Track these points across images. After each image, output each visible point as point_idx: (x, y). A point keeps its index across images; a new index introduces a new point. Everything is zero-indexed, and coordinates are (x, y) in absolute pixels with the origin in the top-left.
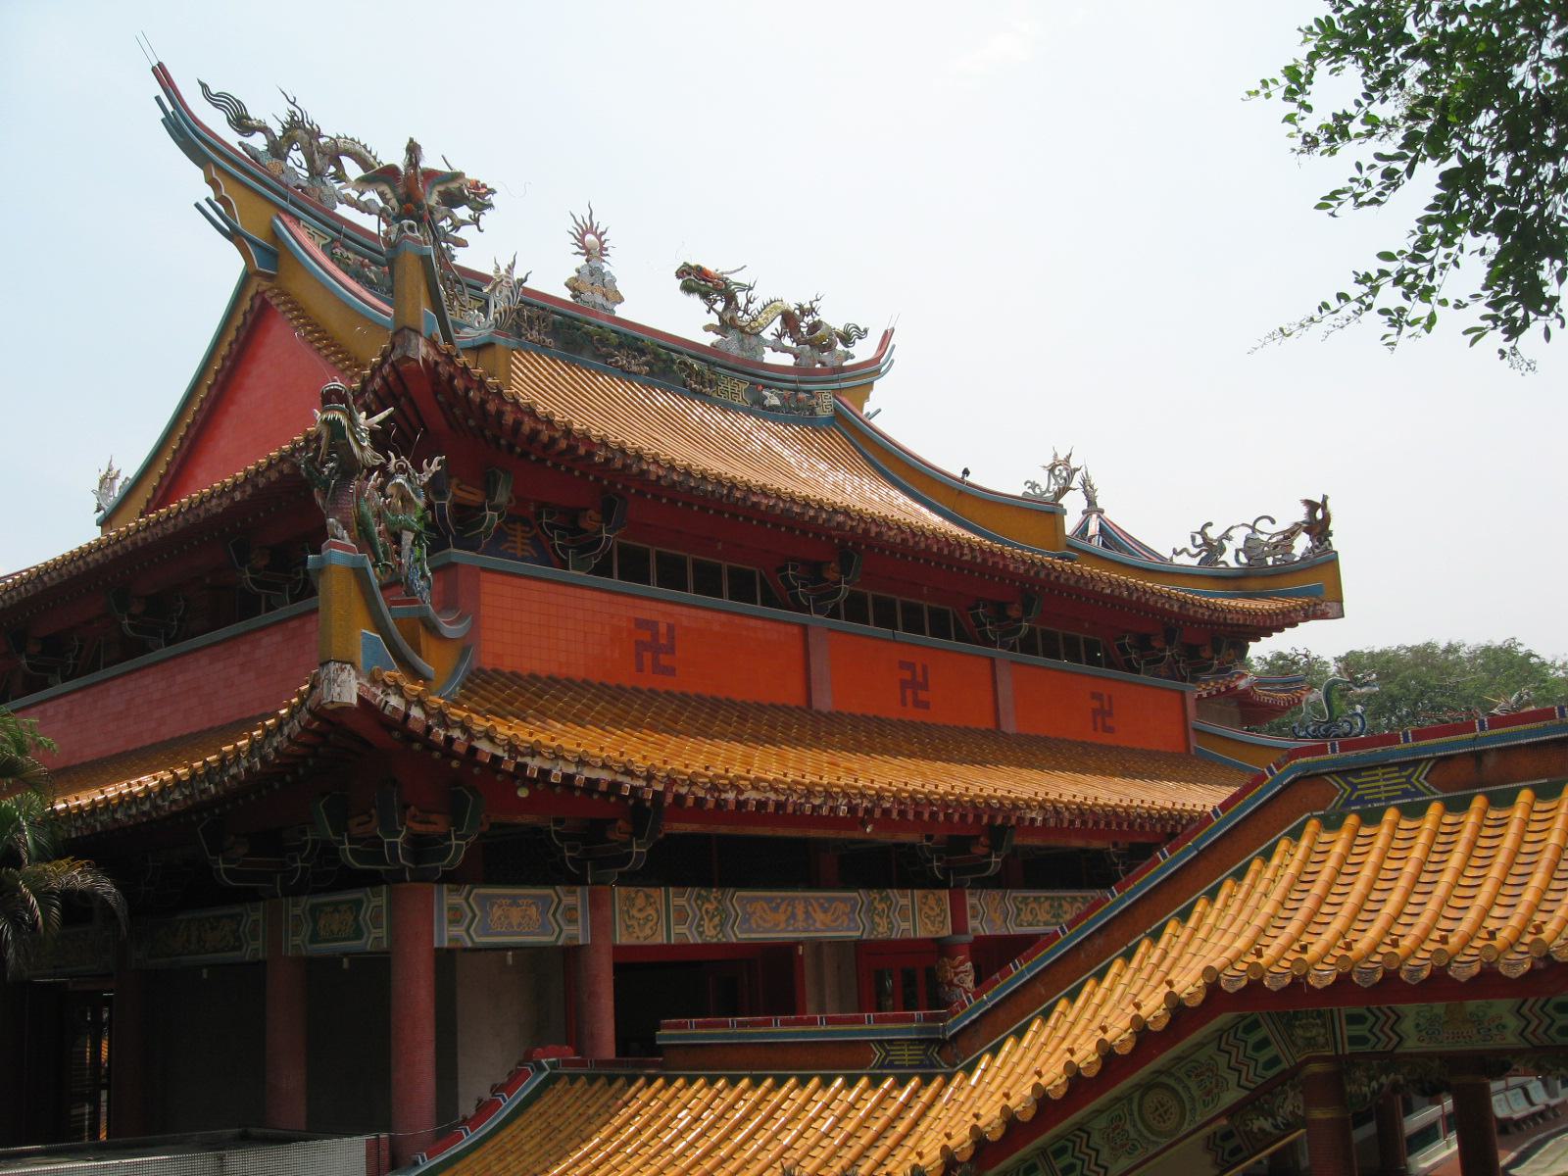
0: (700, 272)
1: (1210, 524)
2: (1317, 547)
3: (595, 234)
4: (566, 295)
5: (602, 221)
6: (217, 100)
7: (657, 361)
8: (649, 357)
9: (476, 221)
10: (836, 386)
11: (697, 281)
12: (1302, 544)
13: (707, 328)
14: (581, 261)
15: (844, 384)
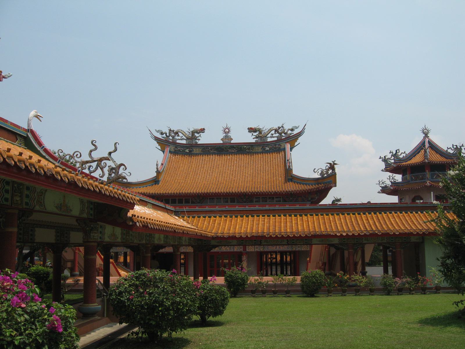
0: (251, 128)
3: (228, 129)
4: (222, 142)
5: (229, 126)
6: (158, 131)
8: (236, 149)
9: (200, 136)
11: (251, 130)
13: (254, 138)
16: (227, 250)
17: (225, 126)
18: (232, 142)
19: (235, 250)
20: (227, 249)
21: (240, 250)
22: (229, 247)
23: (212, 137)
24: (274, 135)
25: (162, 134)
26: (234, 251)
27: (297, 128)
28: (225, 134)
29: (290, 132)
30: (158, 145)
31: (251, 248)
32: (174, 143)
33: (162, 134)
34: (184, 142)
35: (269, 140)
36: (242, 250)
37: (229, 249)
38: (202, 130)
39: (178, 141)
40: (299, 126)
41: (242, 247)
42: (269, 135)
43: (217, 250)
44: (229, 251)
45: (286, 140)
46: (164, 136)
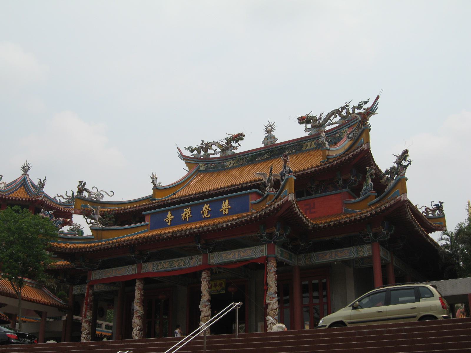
3: (270, 126)
4: (263, 145)
5: (271, 122)
6: (187, 149)
7: (296, 146)
10: (349, 125)
11: (302, 120)
14: (267, 135)
15: (352, 124)
16: (180, 266)
17: (266, 123)
18: (277, 142)
20: (180, 264)
21: (199, 263)
22: (183, 261)
23: (253, 142)
24: (333, 121)
25: (192, 150)
27: (365, 103)
28: (267, 135)
29: (357, 111)
30: (186, 165)
32: (207, 159)
33: (192, 150)
34: (218, 155)
35: (328, 128)
37: (183, 263)
38: (239, 137)
39: (211, 156)
40: (368, 100)
42: (329, 121)
43: (166, 268)
44: (183, 267)
45: (349, 124)
46: (196, 152)
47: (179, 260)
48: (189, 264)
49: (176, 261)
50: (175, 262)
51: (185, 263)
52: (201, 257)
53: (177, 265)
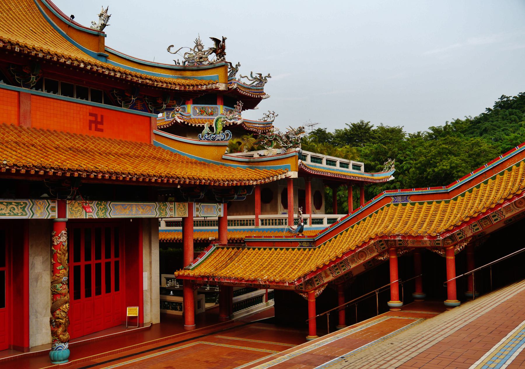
1: (172, 46)
2: (218, 59)
12: (213, 57)
16: (15, 215)
19: (38, 216)
22: (19, 207)
26: (35, 217)
31: (78, 211)
36: (57, 217)
37: (21, 211)
41: (55, 207)
47: (11, 203)
48: (33, 214)
49: (6, 204)
50: (2, 205)
51: (24, 210)
52: (56, 205)
53: (8, 211)
